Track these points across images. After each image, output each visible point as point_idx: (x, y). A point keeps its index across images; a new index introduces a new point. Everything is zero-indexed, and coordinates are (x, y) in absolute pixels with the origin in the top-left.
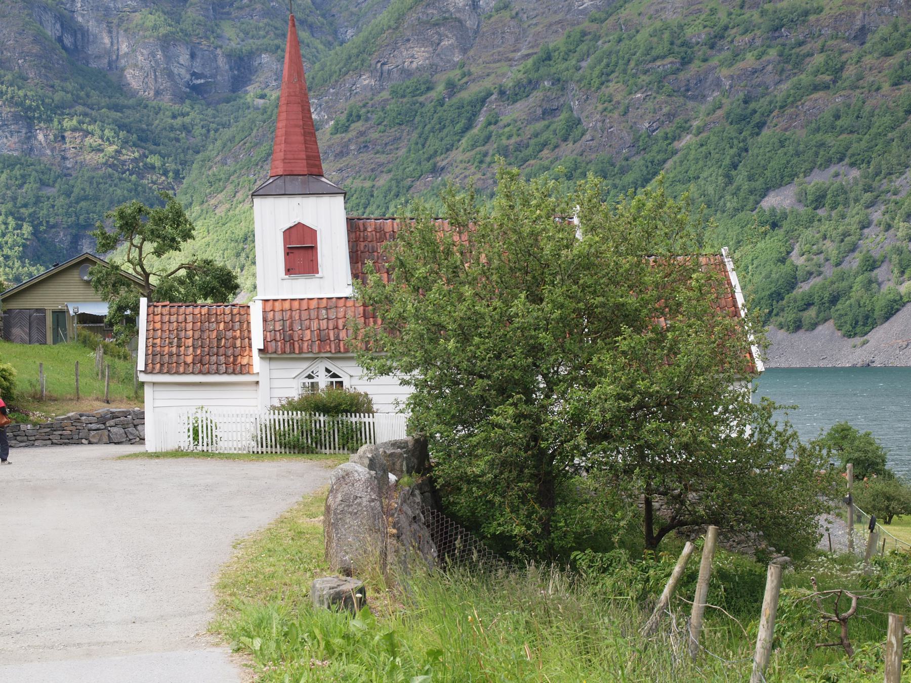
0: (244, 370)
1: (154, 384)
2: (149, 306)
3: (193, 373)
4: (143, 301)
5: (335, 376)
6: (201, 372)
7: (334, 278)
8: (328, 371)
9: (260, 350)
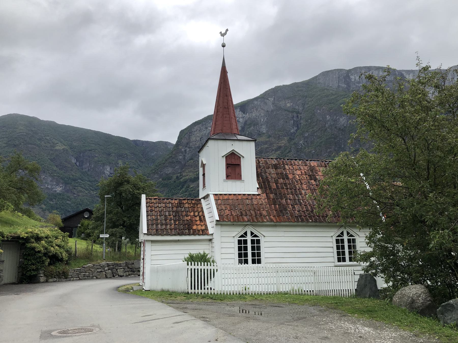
0: (205, 232)
1: (152, 242)
2: (146, 199)
3: (175, 235)
4: (144, 197)
5: (256, 236)
6: (179, 234)
7: (248, 185)
8: (252, 233)
9: (217, 221)
